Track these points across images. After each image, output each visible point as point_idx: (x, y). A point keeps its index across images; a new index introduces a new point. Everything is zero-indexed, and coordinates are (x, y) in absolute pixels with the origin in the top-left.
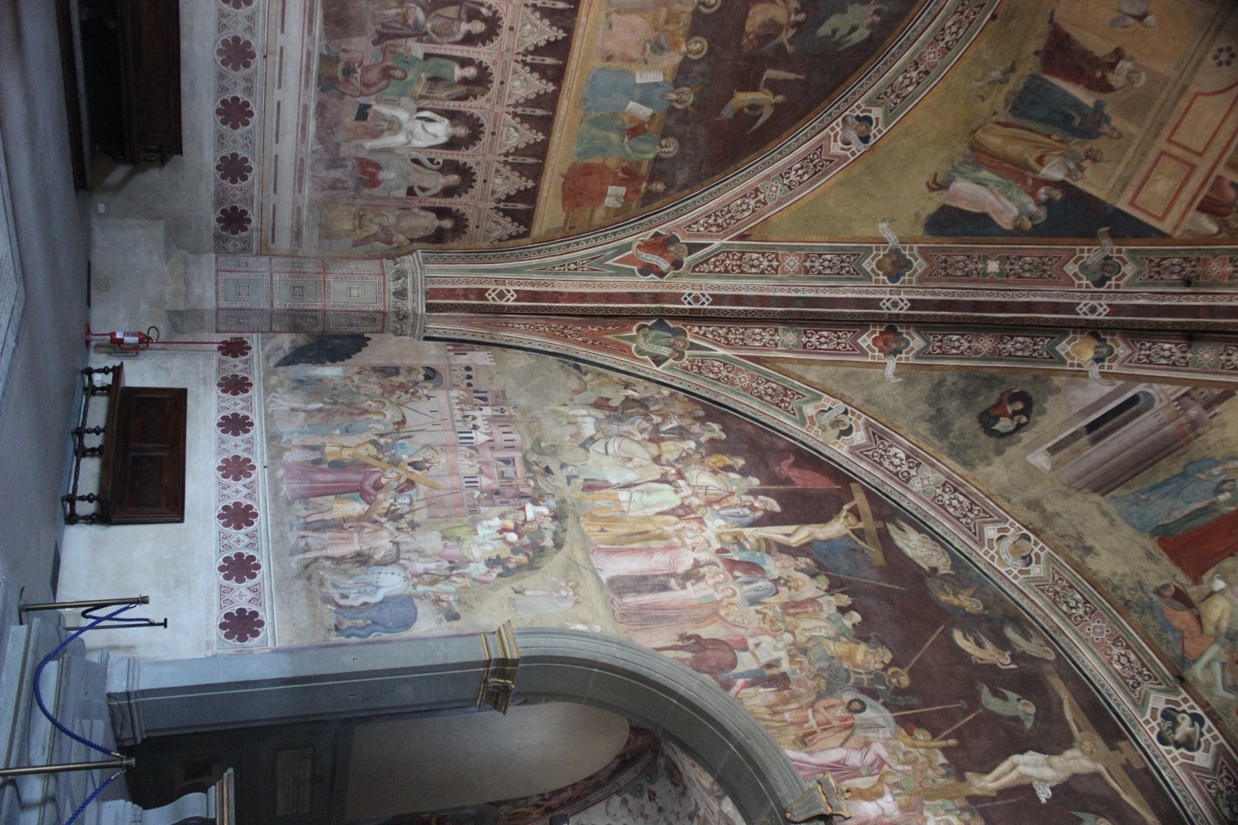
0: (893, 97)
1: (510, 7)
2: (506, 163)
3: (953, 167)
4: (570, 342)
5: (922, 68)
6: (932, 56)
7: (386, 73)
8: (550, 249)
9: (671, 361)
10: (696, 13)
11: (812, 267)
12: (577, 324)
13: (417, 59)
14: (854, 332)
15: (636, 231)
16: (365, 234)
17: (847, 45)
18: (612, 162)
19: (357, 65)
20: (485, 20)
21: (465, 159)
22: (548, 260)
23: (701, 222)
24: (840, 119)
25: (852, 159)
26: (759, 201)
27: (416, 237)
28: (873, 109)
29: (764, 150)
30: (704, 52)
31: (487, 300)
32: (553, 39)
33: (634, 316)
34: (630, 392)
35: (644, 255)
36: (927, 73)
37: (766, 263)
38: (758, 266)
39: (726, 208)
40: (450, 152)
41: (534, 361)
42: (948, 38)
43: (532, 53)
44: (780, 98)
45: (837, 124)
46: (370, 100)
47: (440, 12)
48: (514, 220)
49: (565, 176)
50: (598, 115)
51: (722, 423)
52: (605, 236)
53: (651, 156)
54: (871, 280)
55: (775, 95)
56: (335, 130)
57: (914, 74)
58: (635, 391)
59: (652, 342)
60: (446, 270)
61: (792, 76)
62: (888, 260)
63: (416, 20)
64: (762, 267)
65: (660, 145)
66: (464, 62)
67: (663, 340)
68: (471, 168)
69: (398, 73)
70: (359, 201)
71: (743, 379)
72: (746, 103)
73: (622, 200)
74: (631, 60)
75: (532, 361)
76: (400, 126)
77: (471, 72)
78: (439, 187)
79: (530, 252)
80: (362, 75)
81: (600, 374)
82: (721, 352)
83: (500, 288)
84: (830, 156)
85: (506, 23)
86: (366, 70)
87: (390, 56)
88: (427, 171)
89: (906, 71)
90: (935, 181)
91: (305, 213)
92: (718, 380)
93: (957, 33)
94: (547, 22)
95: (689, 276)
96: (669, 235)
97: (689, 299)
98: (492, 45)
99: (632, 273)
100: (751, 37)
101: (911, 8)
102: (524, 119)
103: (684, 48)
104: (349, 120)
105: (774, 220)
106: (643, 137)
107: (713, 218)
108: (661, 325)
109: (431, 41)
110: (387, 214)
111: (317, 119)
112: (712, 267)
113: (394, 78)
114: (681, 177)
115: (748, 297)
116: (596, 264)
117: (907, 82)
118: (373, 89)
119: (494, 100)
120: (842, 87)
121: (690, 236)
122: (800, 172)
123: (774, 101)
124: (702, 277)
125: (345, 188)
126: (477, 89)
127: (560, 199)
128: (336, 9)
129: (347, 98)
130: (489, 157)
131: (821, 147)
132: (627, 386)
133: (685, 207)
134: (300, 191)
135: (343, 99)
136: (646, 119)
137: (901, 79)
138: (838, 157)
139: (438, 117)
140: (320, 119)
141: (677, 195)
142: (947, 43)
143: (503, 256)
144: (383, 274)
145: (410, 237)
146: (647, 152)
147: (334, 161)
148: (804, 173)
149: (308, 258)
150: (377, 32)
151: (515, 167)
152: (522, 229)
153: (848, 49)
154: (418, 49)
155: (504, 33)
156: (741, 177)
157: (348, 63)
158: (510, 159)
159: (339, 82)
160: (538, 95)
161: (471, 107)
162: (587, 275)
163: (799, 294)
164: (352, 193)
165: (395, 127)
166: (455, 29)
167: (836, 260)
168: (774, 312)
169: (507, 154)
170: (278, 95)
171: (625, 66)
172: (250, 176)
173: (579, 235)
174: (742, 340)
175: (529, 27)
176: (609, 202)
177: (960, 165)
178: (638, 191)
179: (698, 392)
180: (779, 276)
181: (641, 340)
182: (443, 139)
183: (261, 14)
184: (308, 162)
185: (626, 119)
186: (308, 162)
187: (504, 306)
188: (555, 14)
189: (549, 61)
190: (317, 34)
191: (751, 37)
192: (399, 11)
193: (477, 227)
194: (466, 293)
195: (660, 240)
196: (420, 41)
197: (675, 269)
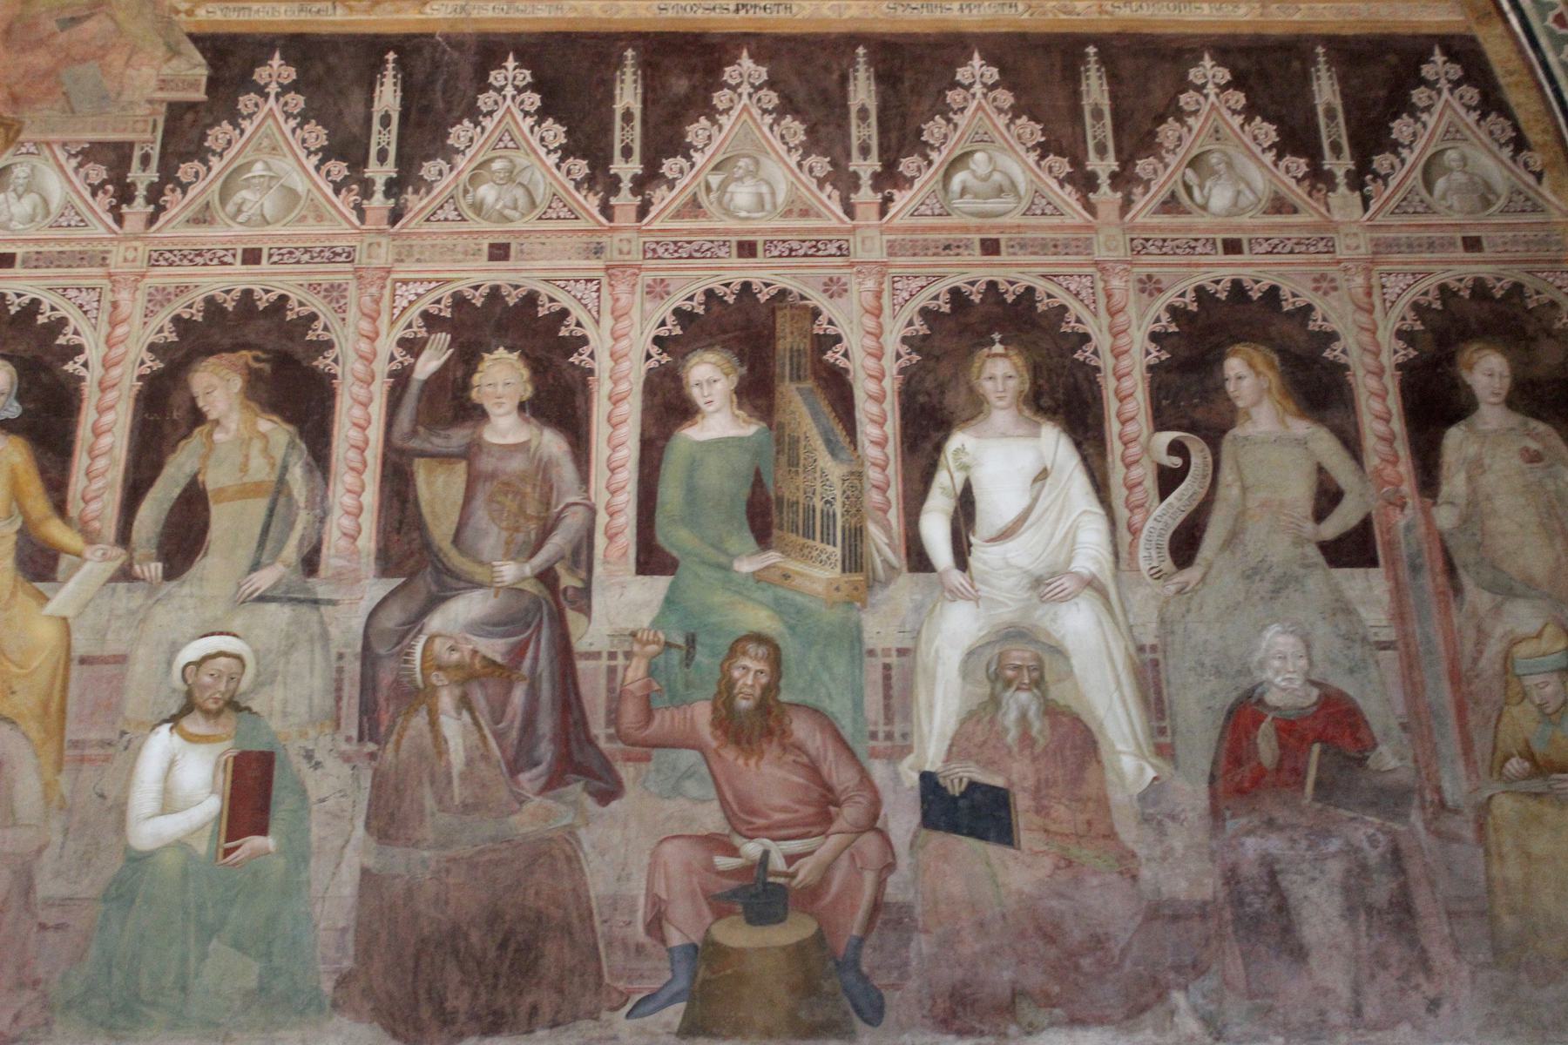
13: (670, 602)
20: (467, 356)
21: (1138, 338)
32: (533, 100)
40: (1111, 406)
43: (598, 157)
47: (441, 531)
48: (1399, 104)
56: (1077, 935)
63: (489, 626)
68: (1173, 311)
69: (750, 673)
70: (1455, 784)
76: (1015, 634)
78: (1301, 427)
80: (776, 831)
87: (664, 721)
88: (1229, 491)
94: (460, 134)
98: (577, 312)
109: (582, 554)
110: (1494, 648)
113: (771, 688)
118: (842, 776)
119: (829, 267)
125: (1396, 858)
126: (788, 339)
128: (453, 976)
130: (1109, 244)
135: (906, 908)
139: (945, 483)
140: (1027, 1011)
147: (1250, 926)
152: (1437, 66)
157: (720, 905)
159: (819, 939)
160: (788, 106)
164: (1416, 818)
165: (1020, 655)
166: (516, 464)
169: (1084, 182)
175: (487, 192)
182: (1053, 444)
188: (426, 110)
189: (628, 95)
192: (446, 700)
193: (1472, 244)
196: (583, 599)
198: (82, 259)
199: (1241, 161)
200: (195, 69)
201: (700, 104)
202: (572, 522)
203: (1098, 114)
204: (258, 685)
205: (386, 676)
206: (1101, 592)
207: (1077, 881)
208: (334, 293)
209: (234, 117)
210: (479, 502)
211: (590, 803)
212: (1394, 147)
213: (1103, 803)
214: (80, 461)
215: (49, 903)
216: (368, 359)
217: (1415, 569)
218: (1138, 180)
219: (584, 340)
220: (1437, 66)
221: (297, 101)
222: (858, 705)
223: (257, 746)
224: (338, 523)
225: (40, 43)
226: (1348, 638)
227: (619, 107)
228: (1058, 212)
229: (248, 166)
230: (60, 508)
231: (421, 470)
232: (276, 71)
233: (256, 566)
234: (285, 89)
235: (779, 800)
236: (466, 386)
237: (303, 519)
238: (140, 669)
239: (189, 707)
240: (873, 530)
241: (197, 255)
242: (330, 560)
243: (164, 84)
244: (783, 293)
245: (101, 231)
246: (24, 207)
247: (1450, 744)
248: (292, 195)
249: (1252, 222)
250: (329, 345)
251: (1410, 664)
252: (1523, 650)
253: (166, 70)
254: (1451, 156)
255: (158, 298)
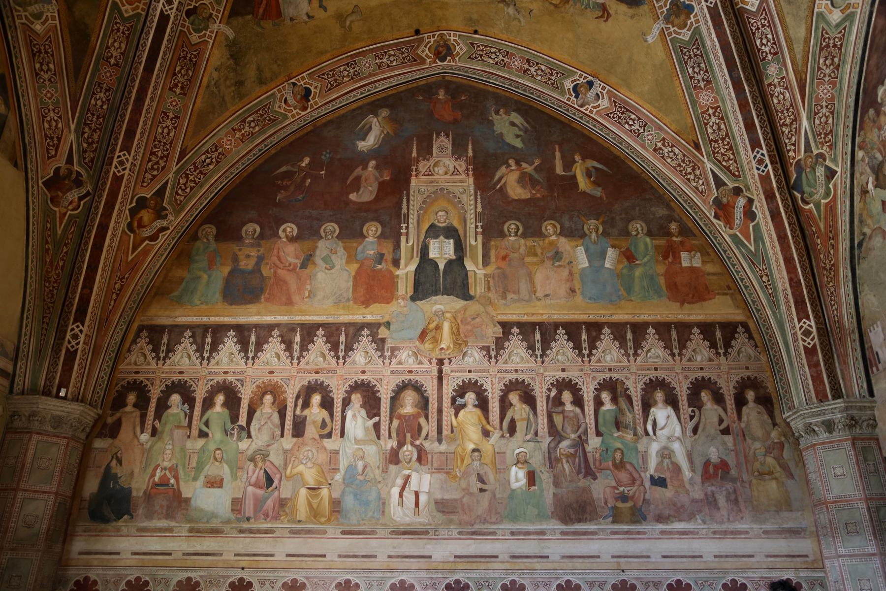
0: (553, 78)
1: (546, 374)
2: (680, 354)
3: (586, 8)
4: (837, 260)
5: (526, 66)
6: (516, 63)
7: (620, 466)
8: (754, 302)
9: (828, 163)
10: (524, 236)
11: (703, 80)
12: (818, 259)
13: (602, 442)
14: (748, 18)
15: (717, 234)
16: (778, 468)
17: (526, 124)
18: (661, 269)
19: (616, 491)
20: (560, 392)
21: (685, 388)
22: (764, 301)
23: (695, 184)
24: (582, 109)
25: (608, 87)
26: (663, 145)
27: (770, 421)
28: (566, 88)
29: (622, 156)
30: (553, 222)
31: (815, 345)
32: (566, 337)
33: (795, 211)
34: (870, 186)
35: (737, 221)
36: (528, 61)
37: (713, 119)
38: (718, 124)
39: (678, 169)
40: (680, 402)
41: (865, 285)
42: (501, 58)
43: (580, 351)
44: (577, 158)
45: (586, 110)
46: (646, 476)
47: (559, 428)
48: (733, 338)
49: (682, 304)
50: (622, 289)
51: (875, 88)
52: (729, 258)
53: (648, 239)
54: (698, 26)
55: (576, 162)
56: (679, 505)
57: (532, 70)
58: (867, 183)
59: (815, 187)
60: (797, 388)
61: (558, 154)
62: (676, 21)
63: (570, 447)
64: (717, 121)
65: (637, 235)
66: (598, 403)
67: (810, 177)
69: (618, 455)
70: (745, 477)
71: (824, 91)
72: (587, 180)
73: (693, 253)
74: (571, 274)
75: (866, 288)
76: (665, 448)
77: (605, 396)
78: (716, 407)
79: (761, 318)
80: (625, 486)
81: (861, 222)
82: (805, 123)
83: (800, 336)
84: (611, 105)
85: (560, 375)
86: (619, 483)
87: (604, 465)
88: (703, 420)
89: (532, 77)
90: (602, 17)
91: (768, 527)
92: (832, 113)
93: (495, 53)
94: (553, 344)
95: (745, 177)
96: (714, 207)
97: (762, 168)
98: (579, 383)
99: (757, 228)
100: (534, 192)
101: (489, 91)
102: (637, 346)
103: (554, 238)
104: (667, 493)
105: (674, 127)
106: (633, 251)
107: (689, 176)
108: (797, 186)
109: (585, 432)
111: (672, 522)
112: (731, 162)
113: (622, 459)
114: (661, 212)
115: (744, 120)
116: (757, 259)
117: (539, 72)
118: (636, 476)
119: (626, 373)
120: (558, 117)
121: (710, 190)
122: (631, 122)
123: (580, 161)
124: (742, 166)
125: (735, 491)
127: (704, 303)
129: (647, 496)
130: (678, 369)
131: (607, 115)
132: (865, 192)
133: (685, 201)
134: (747, 533)
135: (649, 500)
136: (617, 251)
137: (539, 78)
138: (610, 99)
139: (651, 418)
140: (671, 519)
141: (678, 211)
142: (504, 57)
143: (770, 341)
144: (813, 446)
145: (772, 426)
146: (645, 244)
148: (631, 119)
149: (815, 521)
150: (585, 477)
151: (682, 346)
152: (740, 329)
153: (527, 122)
154: (594, 442)
155: (567, 375)
156: (648, 166)
158: (676, 351)
159: (634, 505)
160: (615, 339)
161: (636, 391)
162: (769, 265)
163: (728, 78)
164: (739, 484)
165: (666, 452)
166: (572, 414)
167: (690, 63)
168: (750, 92)
169: (673, 355)
170: (656, 558)
171: (577, 276)
172: (741, 581)
173: (734, 281)
174: (788, 110)
175: (559, 357)
176: (697, 262)
177: (583, 4)
178: (682, 243)
179: (851, 125)
180: (720, 104)
181: (816, 197)
182: (670, 410)
183: (586, 576)
184: (715, 527)
185: (621, 266)
186: (715, 527)
187: (818, 329)
188: (546, 339)
189: (584, 336)
190: (596, 527)
191: (534, 192)
192: (564, 461)
193: (747, 368)
194: (814, 365)
195: (721, 213)
197: (742, 191)
198: (484, 371)
199: (703, 350)
200: (499, 329)
201: (598, 338)
202: (583, 426)
203: (675, 340)
204: (530, 458)
205: (553, 456)
206: (680, 440)
207: (679, 495)
208: (533, 379)
209: (509, 340)
210: (566, 422)
211: (592, 481)
212: (732, 347)
213: (683, 480)
214: (491, 413)
215: (499, 499)
216: (541, 393)
217: (737, 435)
218: (683, 354)
219: (581, 389)
220: (740, 329)
221: (520, 337)
222: (638, 462)
223: (531, 470)
224: (540, 426)
225: (468, 324)
226: (725, 449)
227: (583, 339)
228: (668, 362)
229: (513, 351)
230: (488, 423)
231: (554, 415)
232: (515, 330)
233: (526, 435)
234: (518, 334)
235: (625, 480)
236: (560, 398)
237: (534, 425)
238: (509, 453)
239: (518, 462)
240: (638, 428)
241: (506, 371)
242: (540, 434)
243: (494, 333)
244: (618, 379)
245: (487, 365)
246: (471, 360)
247: (744, 470)
248: (522, 358)
249: (705, 363)
250: (534, 390)
251: (737, 454)
252: (757, 451)
253: (494, 330)
254: (743, 349)
255: (500, 379)
